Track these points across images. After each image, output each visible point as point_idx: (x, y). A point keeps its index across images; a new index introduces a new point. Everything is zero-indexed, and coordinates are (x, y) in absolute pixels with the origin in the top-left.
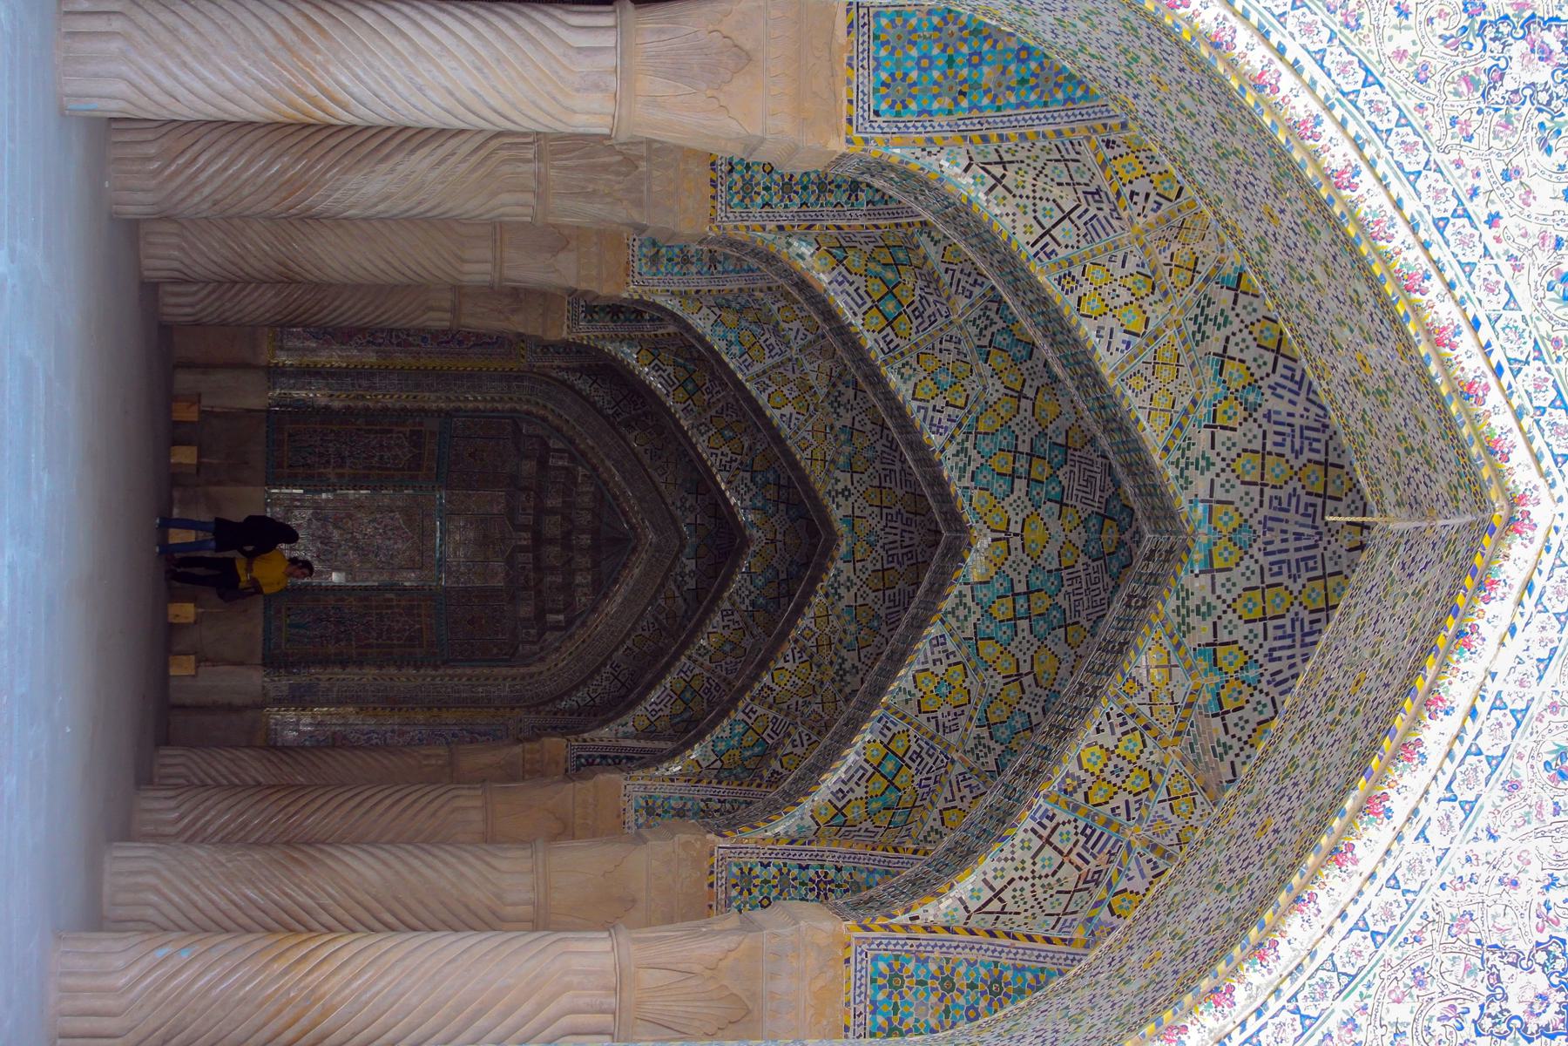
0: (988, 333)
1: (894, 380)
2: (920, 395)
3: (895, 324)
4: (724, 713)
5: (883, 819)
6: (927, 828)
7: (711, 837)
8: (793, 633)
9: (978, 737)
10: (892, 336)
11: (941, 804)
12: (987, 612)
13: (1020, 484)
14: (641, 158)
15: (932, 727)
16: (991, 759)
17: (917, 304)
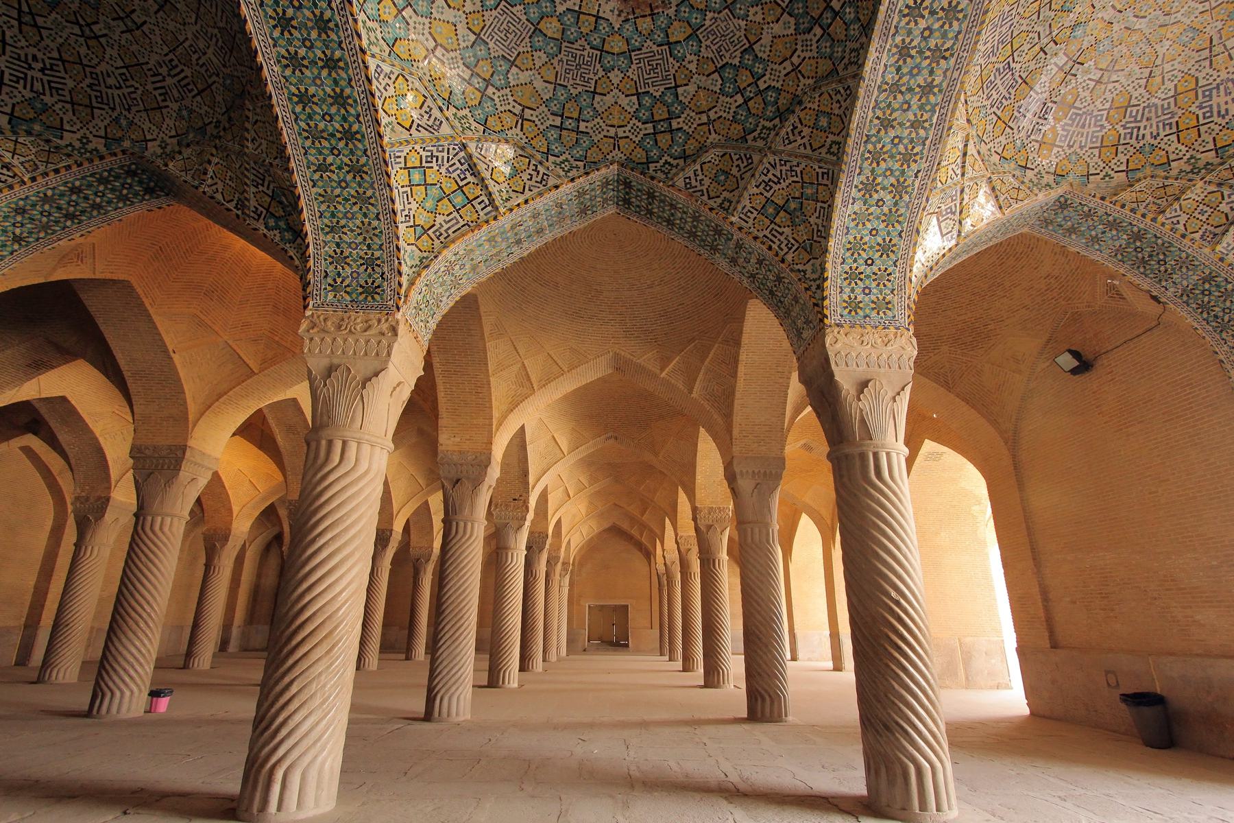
5: (445, 206)
15: (424, 134)
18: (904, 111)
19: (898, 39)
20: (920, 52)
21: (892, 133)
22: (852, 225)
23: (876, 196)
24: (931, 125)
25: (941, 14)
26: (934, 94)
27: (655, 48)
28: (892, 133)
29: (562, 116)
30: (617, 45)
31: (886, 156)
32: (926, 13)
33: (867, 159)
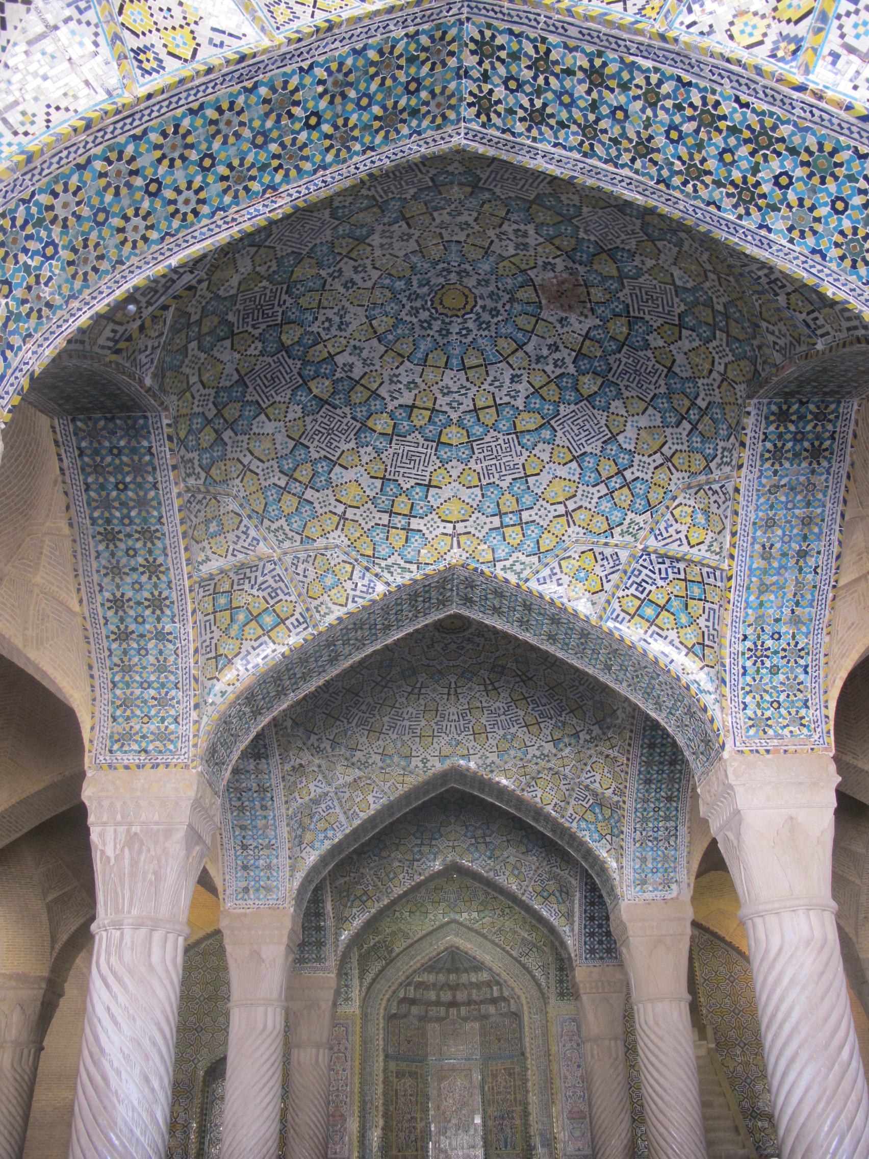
0: (290, 534)
1: (331, 619)
2: (343, 601)
3: (283, 616)
4: (573, 838)
5: (696, 607)
6: (708, 555)
7: (726, 755)
8: (518, 792)
9: (622, 534)
10: (293, 620)
11: (685, 548)
12: (517, 548)
13: (415, 524)
14: (128, 831)
15: (615, 578)
16: (640, 519)
17: (265, 594)
18: (627, 117)
19: (520, 127)
20: (539, 92)
21: (660, 141)
22: (810, 241)
23: (766, 188)
24: (656, 70)
25: (486, 65)
26: (605, 64)
27: (626, 291)
28: (660, 141)
29: (683, 418)
30: (619, 328)
31: (697, 157)
32: (486, 87)
33: (695, 191)
